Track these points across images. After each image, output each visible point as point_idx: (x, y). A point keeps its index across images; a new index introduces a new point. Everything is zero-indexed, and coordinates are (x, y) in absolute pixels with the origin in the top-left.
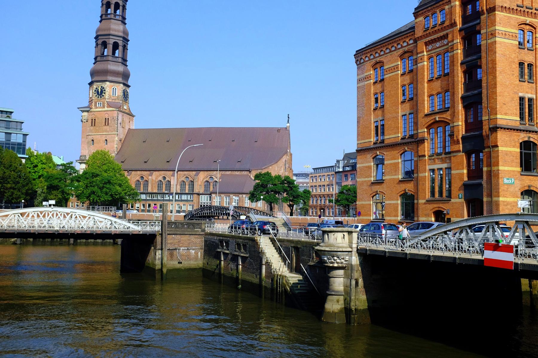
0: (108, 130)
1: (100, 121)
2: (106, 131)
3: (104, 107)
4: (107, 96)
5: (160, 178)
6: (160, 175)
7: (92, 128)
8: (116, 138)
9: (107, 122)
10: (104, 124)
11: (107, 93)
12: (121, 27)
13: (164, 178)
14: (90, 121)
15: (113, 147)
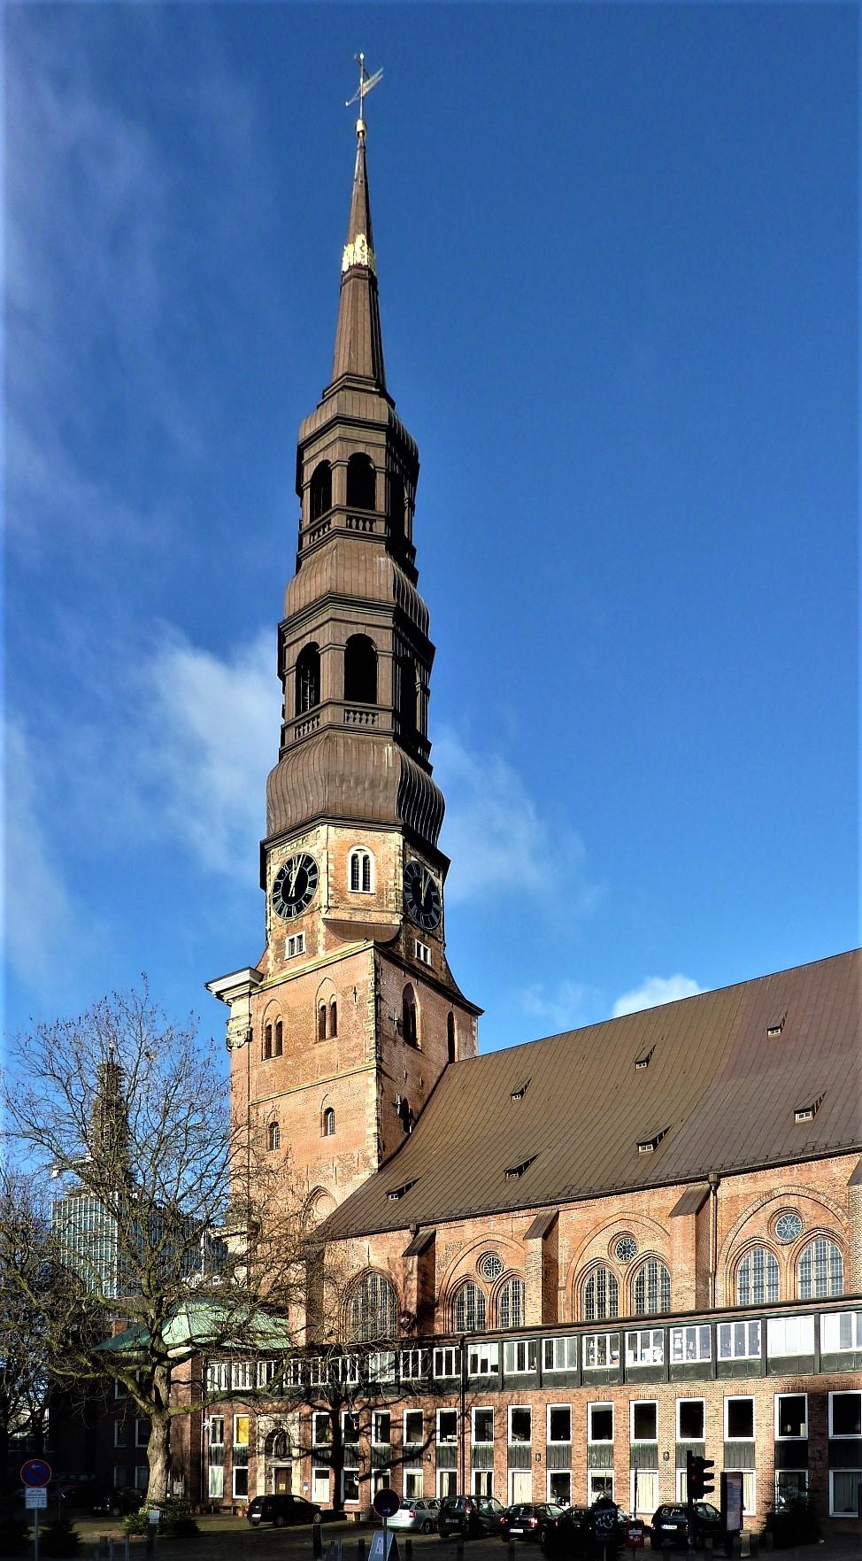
0: (335, 1057)
1: (300, 1027)
2: (328, 1067)
3: (313, 952)
4: (321, 895)
5: (599, 1248)
6: (599, 1227)
7: (268, 1065)
8: (373, 1093)
9: (328, 1022)
10: (314, 1034)
11: (323, 880)
12: (375, 573)
13: (624, 1247)
14: (259, 1038)
15: (359, 1140)
